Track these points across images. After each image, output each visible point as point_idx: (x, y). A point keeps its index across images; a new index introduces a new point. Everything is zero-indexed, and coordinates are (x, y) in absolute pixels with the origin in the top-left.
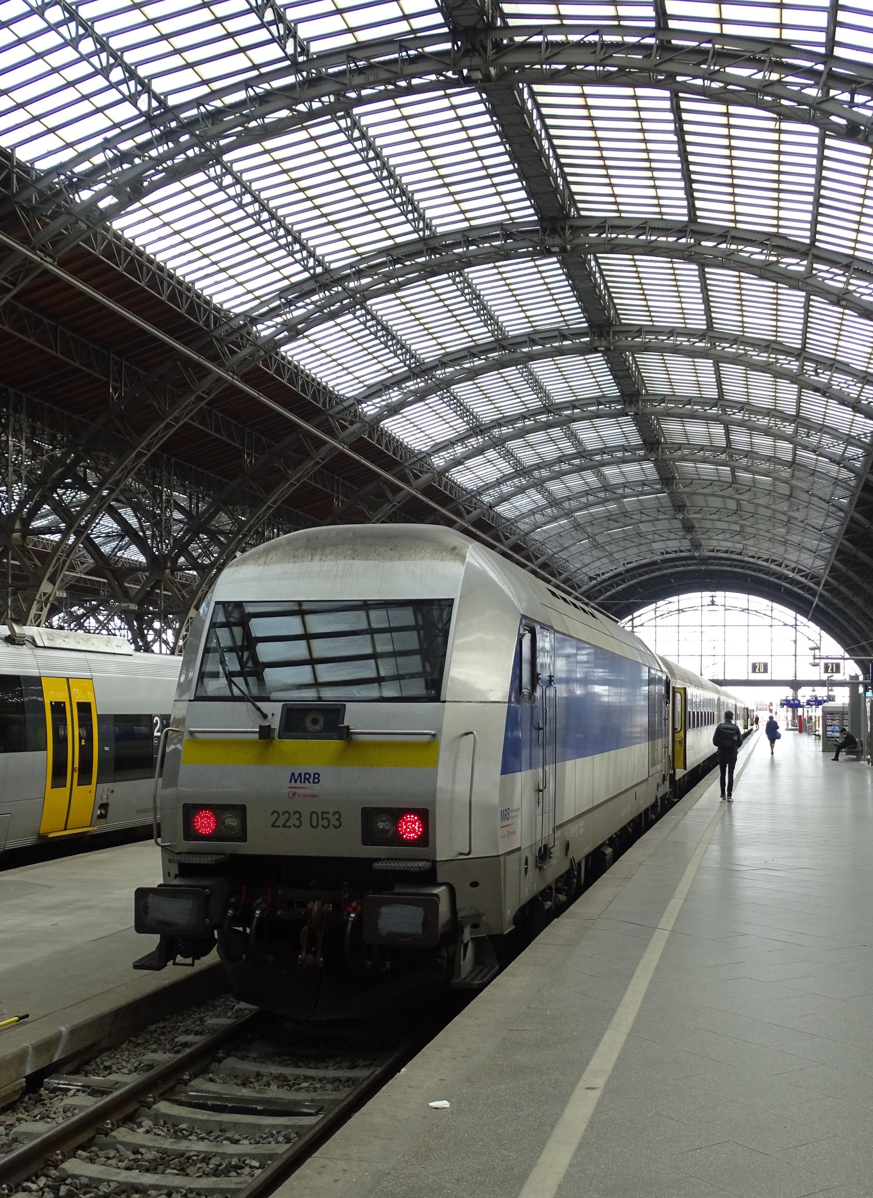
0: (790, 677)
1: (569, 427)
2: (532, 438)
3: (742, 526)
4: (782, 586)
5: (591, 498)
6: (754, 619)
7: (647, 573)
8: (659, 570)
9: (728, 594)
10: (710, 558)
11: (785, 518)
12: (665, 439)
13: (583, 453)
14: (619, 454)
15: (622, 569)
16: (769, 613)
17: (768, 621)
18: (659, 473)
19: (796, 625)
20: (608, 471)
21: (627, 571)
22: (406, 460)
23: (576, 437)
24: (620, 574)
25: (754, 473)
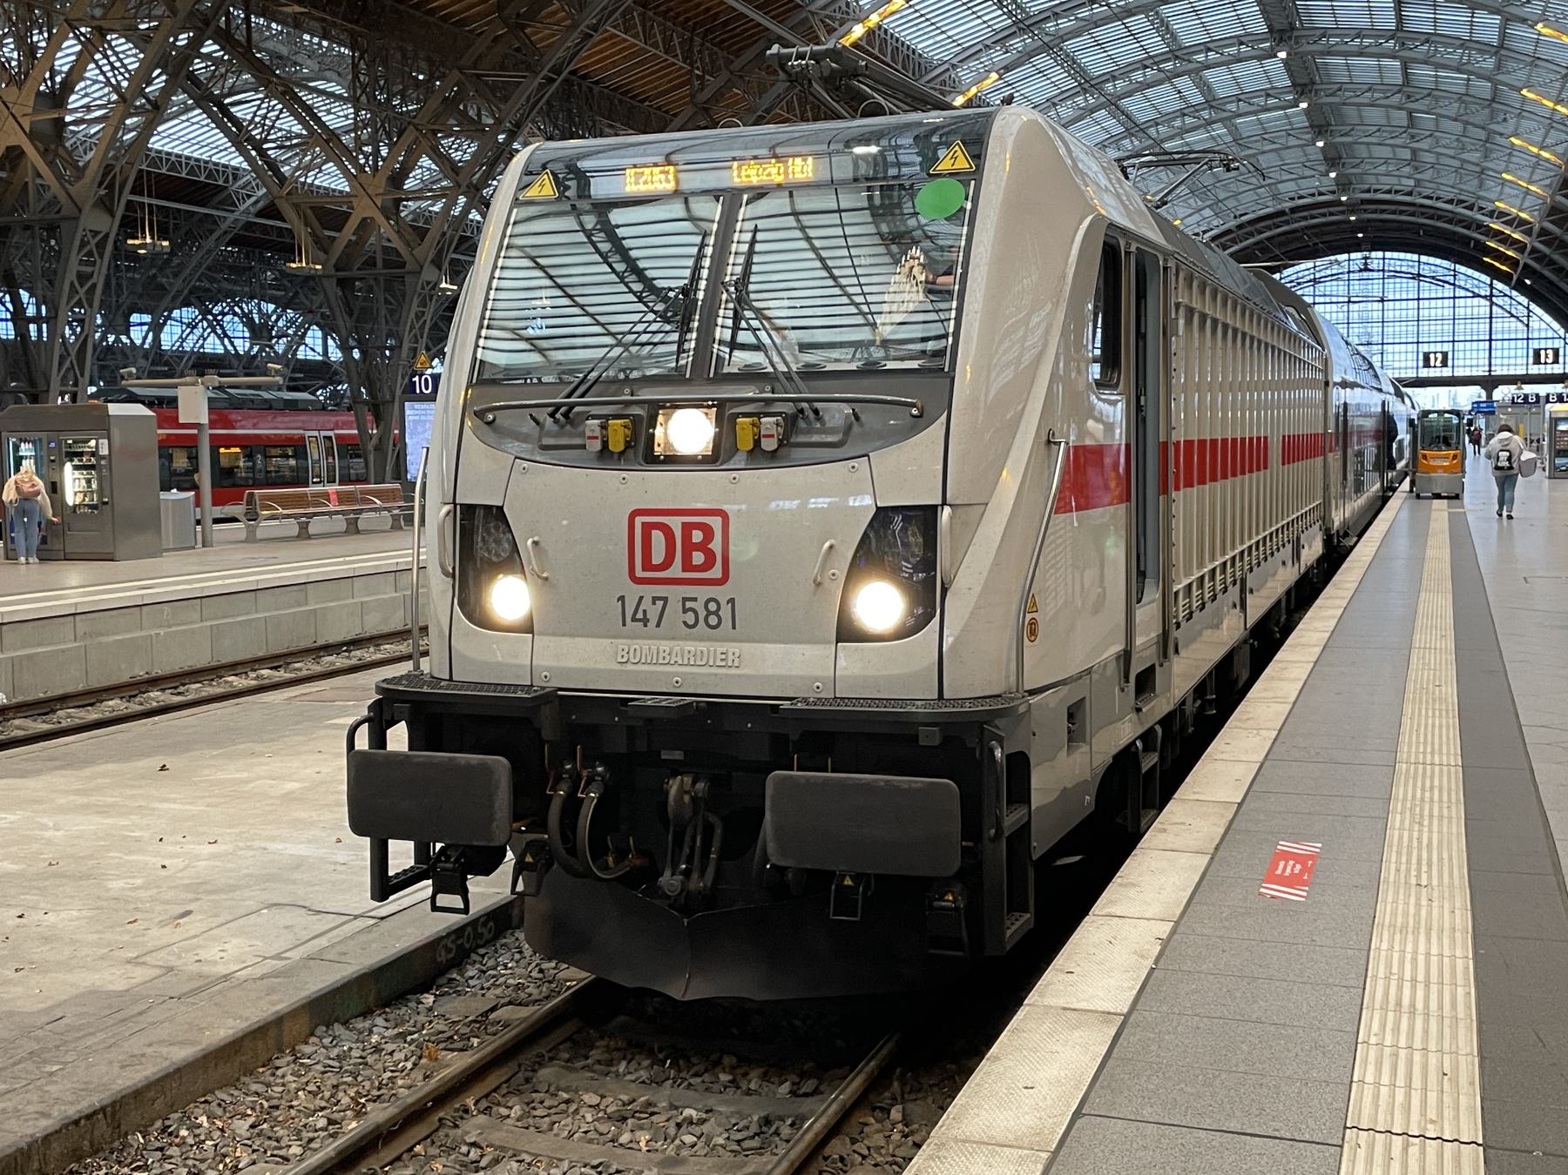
0: (1481, 372)
1: (1157, 13)
2: (1101, 32)
3: (1414, 152)
4: (1470, 238)
5: (1188, 120)
6: (1427, 290)
7: (1269, 228)
8: (1287, 223)
9: (1388, 254)
10: (1363, 202)
11: (1482, 135)
12: (1301, 23)
13: (1177, 52)
14: (1233, 50)
15: (1232, 224)
16: (1451, 279)
17: (1448, 291)
18: (1291, 76)
19: (1492, 295)
20: (1215, 77)
21: (1240, 227)
22: (921, 76)
23: (1167, 28)
24: (1229, 232)
25: (1438, 66)
